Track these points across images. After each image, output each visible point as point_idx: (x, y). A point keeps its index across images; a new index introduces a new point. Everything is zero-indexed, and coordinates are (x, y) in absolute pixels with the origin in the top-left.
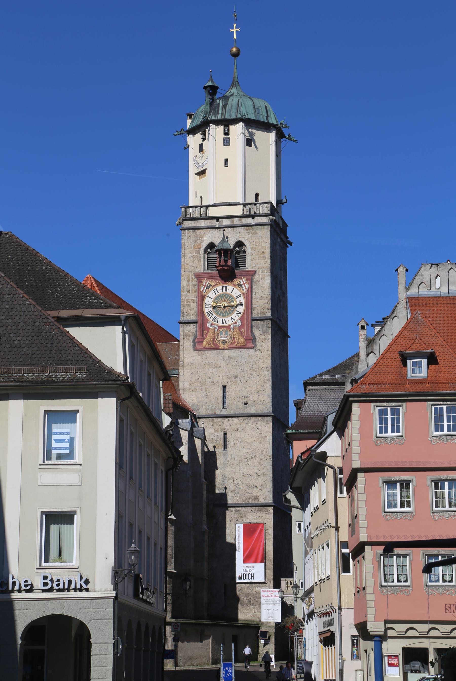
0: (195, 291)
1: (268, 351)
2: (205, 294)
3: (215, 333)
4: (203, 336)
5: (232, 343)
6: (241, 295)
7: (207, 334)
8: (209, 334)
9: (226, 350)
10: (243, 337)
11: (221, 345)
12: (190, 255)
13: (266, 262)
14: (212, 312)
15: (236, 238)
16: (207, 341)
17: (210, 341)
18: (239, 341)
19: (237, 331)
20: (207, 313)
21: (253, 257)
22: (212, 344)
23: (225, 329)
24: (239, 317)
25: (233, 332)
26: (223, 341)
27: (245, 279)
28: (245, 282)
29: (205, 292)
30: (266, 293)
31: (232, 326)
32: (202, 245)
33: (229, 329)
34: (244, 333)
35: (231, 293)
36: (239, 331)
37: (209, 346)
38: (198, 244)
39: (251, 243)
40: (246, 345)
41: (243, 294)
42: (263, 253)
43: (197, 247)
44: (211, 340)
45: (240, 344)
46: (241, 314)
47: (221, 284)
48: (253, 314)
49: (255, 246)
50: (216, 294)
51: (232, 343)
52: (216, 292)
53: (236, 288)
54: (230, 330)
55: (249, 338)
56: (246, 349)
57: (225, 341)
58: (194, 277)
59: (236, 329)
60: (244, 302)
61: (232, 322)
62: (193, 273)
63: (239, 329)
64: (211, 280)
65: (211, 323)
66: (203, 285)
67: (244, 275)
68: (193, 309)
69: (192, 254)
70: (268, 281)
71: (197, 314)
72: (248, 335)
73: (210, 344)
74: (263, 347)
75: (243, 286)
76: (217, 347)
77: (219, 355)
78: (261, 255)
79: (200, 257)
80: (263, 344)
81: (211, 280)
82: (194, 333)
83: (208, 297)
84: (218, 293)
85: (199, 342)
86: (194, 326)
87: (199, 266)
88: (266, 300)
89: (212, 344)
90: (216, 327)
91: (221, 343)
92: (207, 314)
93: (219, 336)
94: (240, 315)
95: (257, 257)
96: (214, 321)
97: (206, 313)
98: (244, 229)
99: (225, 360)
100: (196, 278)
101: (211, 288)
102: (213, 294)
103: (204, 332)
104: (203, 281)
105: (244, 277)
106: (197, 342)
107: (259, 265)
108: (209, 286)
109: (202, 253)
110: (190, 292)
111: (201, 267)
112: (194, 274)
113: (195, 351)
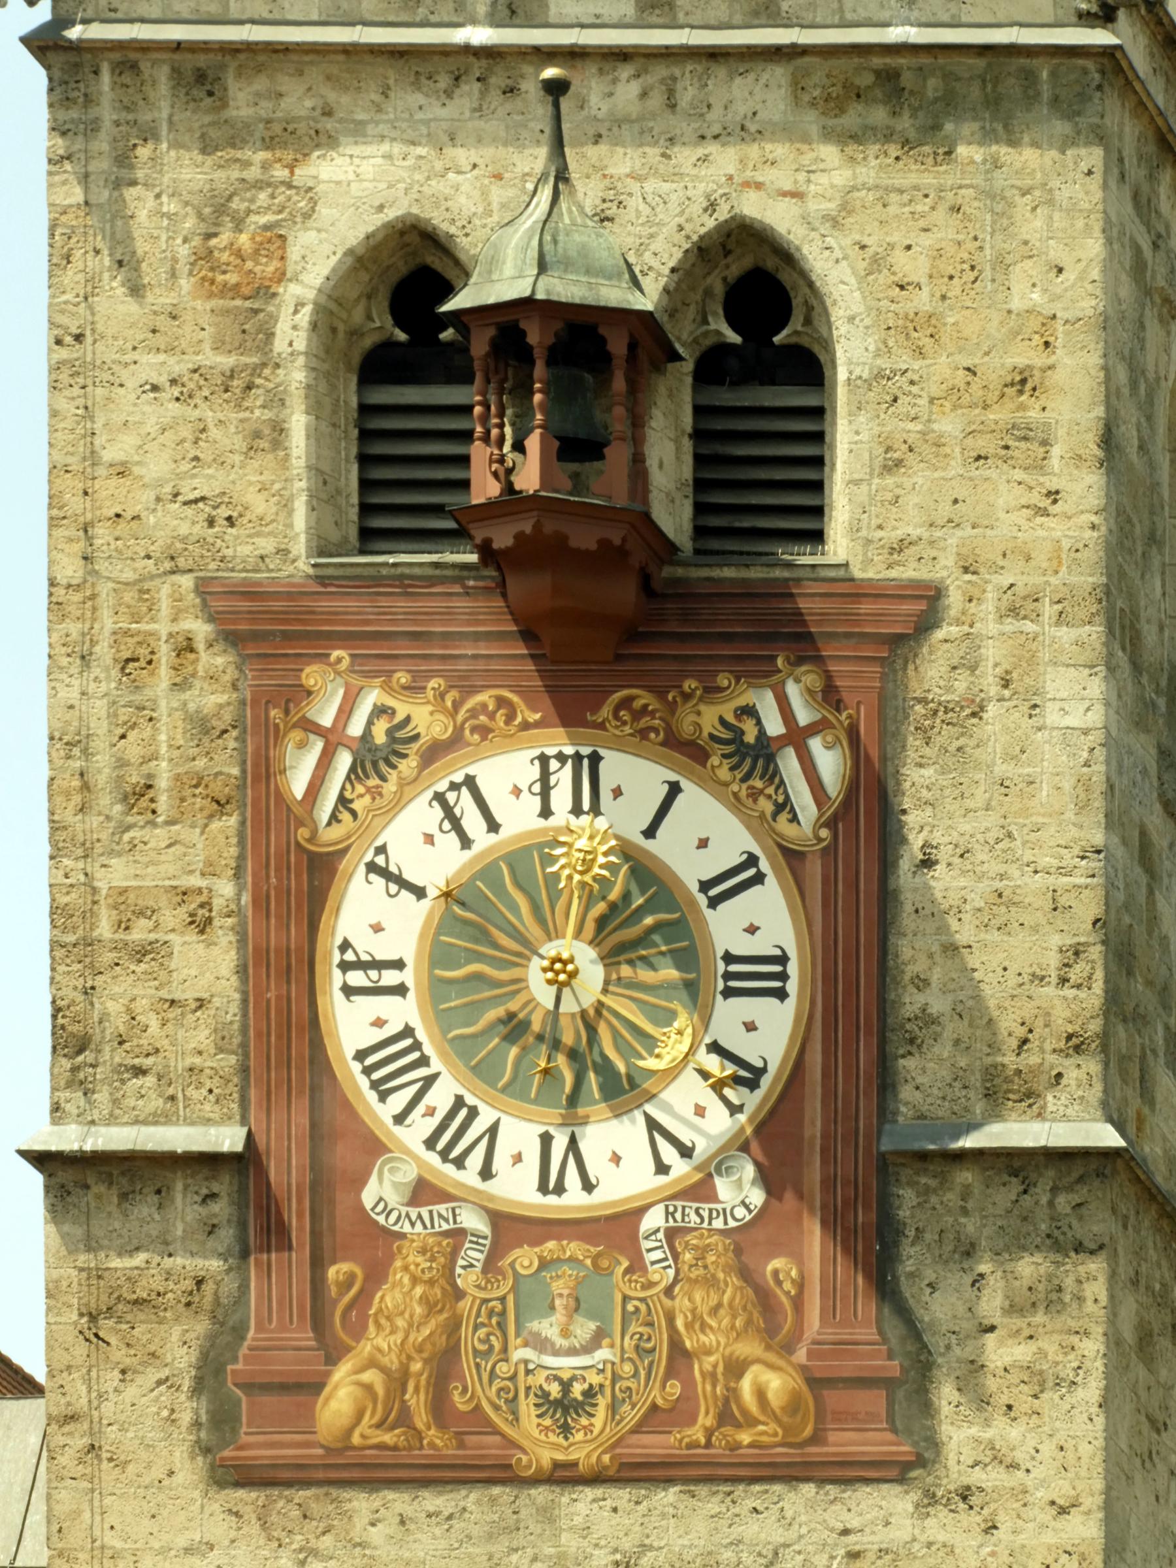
0: (219, 789)
1: (1063, 1511)
2: (336, 832)
3: (459, 1294)
4: (319, 1321)
5: (654, 1407)
6: (764, 865)
8: (388, 1297)
9: (590, 1493)
10: (788, 1348)
13: (1053, 495)
14: (428, 1049)
15: (698, 192)
16: (369, 1376)
17: (398, 1381)
18: (733, 1394)
19: (710, 1282)
20: (360, 1055)
22: (421, 1418)
23: (574, 1248)
25: (669, 1291)
26: (554, 1390)
27: (812, 679)
28: (804, 717)
29: (334, 818)
30: (1046, 861)
31: (654, 1219)
33: (622, 1251)
34: (798, 1302)
35: (650, 833)
36: (735, 1280)
37: (388, 1438)
39: (877, 263)
40: (817, 1438)
42: (1022, 382)
43: (232, 278)
44: (416, 1366)
45: (754, 1422)
46: (766, 1081)
47: (526, 726)
48: (906, 1093)
49: (922, 300)
50: (466, 842)
51: (654, 1407)
52: (473, 822)
53: (701, 782)
54: (637, 1265)
55: (849, 1367)
56: (822, 1482)
57: (577, 1390)
58: (201, 629)
59: (702, 1253)
60: (792, 953)
61: (662, 1168)
62: (186, 582)
63: (738, 1251)
64: (403, 678)
65: (408, 1174)
66: (317, 730)
68: (201, 1003)
69: (170, 350)
70: (1073, 721)
71: (244, 1070)
73: (404, 1419)
74: (1013, 1466)
75: (789, 764)
76: (486, 1446)
78: (1000, 415)
79: (277, 400)
80: (1014, 1433)
81: (403, 678)
82: (209, 1288)
83: (372, 867)
84: (493, 826)
85: (267, 1388)
86: (215, 1207)
87: (260, 505)
88: (1056, 940)
89: (421, 1418)
90: (472, 1220)
91: (527, 1408)
92: (367, 1071)
93: (501, 1326)
95: (949, 425)
96: (444, 1155)
97: (349, 1053)
98: (798, 87)
100: (231, 638)
101: (408, 766)
104: (311, 676)
105: (800, 661)
106: (249, 1387)
107: (969, 531)
108: (380, 737)
109: (301, 345)
110: (163, 803)
111: (291, 513)
112: (203, 588)
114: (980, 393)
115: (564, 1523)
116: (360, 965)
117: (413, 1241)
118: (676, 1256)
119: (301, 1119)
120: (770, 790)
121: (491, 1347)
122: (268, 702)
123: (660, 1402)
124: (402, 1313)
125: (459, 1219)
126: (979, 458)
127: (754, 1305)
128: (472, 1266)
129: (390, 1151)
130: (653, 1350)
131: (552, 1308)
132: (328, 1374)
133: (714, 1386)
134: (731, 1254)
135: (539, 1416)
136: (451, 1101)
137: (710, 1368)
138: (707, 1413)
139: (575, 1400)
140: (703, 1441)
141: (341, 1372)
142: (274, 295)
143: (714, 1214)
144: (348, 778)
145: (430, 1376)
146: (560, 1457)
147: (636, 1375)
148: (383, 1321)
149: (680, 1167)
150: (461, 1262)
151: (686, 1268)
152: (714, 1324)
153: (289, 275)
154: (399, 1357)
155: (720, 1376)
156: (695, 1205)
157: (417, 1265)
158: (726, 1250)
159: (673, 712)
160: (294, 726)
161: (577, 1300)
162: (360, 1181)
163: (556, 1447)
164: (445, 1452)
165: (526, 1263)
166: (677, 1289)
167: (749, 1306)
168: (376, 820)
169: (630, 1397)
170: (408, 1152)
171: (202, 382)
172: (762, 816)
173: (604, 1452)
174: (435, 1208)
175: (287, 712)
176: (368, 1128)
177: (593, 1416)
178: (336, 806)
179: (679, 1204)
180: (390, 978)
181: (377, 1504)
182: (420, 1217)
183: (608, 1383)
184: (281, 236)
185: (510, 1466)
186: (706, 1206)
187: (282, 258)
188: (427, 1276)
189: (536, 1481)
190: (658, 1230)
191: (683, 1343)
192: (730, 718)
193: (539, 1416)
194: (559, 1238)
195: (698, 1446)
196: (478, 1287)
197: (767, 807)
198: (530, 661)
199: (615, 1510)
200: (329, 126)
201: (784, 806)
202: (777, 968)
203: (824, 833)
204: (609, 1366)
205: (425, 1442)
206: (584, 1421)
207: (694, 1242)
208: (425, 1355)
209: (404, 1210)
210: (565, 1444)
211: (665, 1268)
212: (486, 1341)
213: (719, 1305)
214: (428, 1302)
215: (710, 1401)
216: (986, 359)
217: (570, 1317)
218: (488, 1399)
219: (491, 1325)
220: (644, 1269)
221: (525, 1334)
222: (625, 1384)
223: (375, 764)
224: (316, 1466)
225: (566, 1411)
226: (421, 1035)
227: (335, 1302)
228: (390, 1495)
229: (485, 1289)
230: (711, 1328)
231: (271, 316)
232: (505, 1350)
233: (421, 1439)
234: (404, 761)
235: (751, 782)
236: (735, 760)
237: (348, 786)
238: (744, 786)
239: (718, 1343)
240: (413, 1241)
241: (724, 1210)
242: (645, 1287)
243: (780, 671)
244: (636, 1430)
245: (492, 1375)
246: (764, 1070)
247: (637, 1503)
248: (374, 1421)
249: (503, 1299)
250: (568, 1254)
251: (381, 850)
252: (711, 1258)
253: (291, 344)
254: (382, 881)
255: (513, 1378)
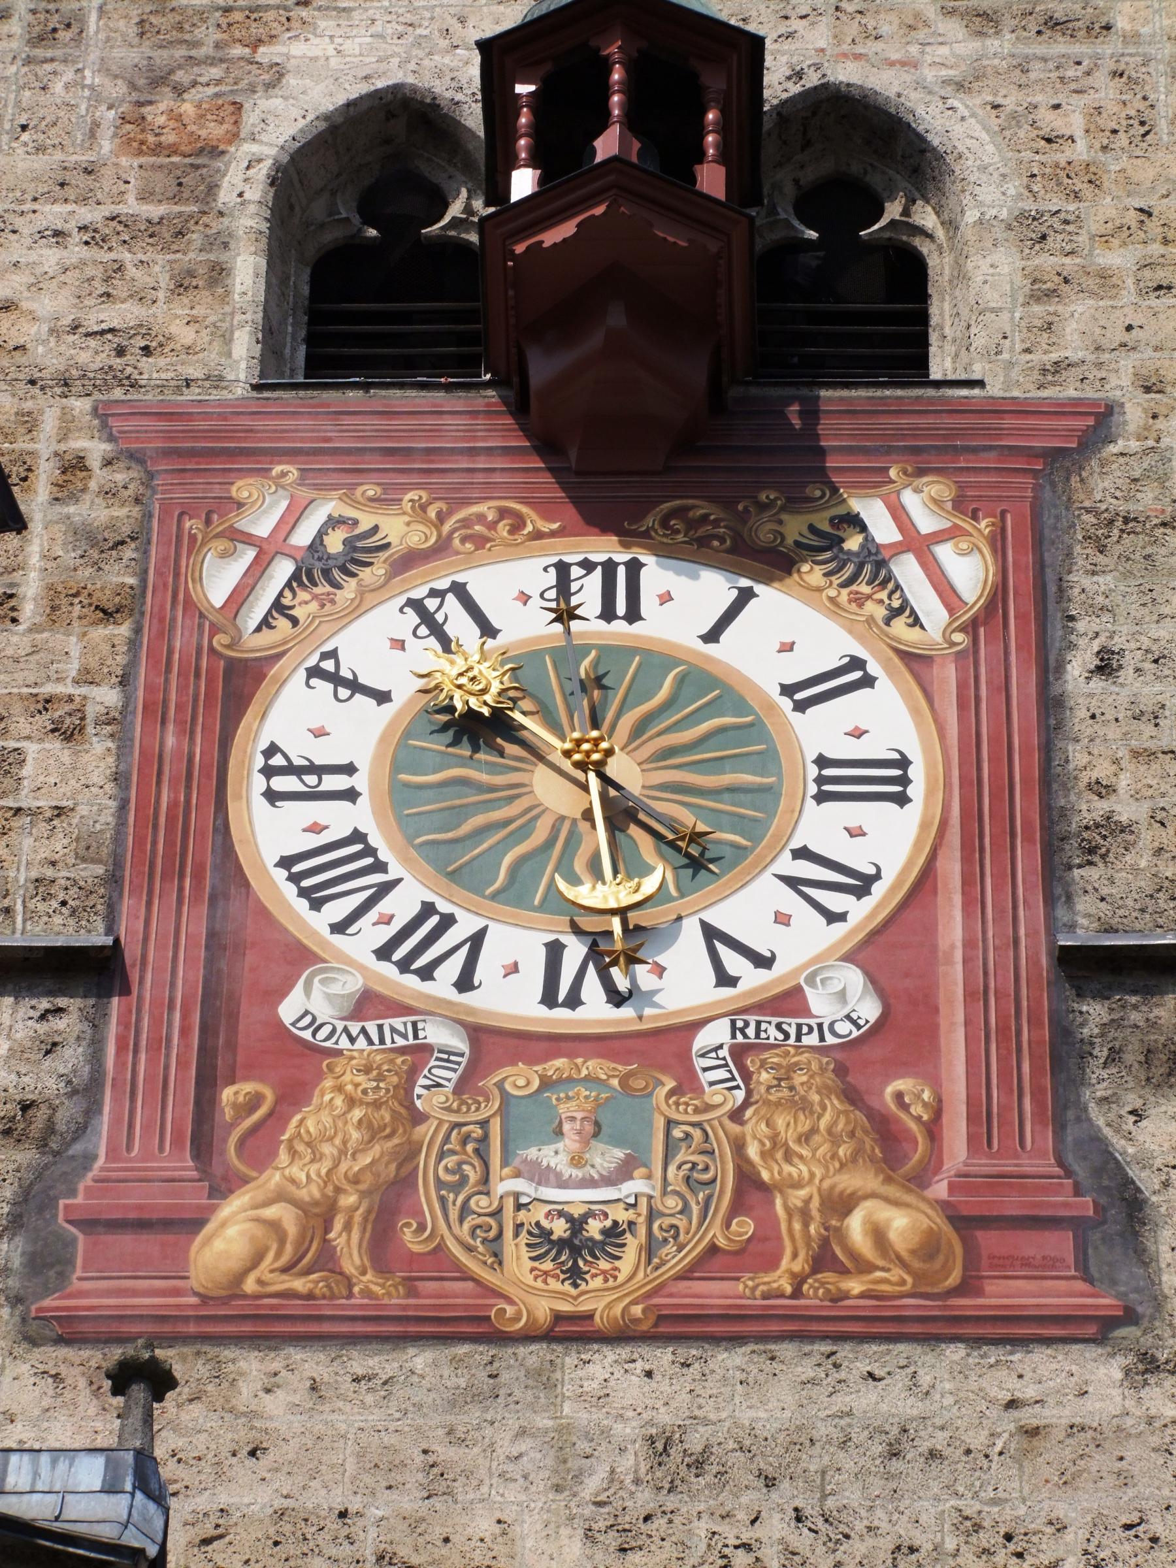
2: (267, 638)
3: (418, 1118)
5: (713, 1249)
7: (277, 1118)
9: (610, 1354)
11: (529, 1279)
12: (53, 214)
16: (271, 1212)
20: (286, 862)
21: (1047, 262)
23: (593, 1066)
24: (839, 929)
25: (736, 1115)
27: (939, 488)
29: (265, 623)
31: (717, 1034)
32: (250, 119)
33: (664, 1069)
35: (712, 636)
37: (300, 1285)
38: (188, 109)
41: (903, 655)
43: (169, 138)
44: (349, 1200)
45: (863, 1267)
46: (878, 889)
49: (1081, 151)
51: (713, 1249)
54: (688, 1083)
57: (594, 1228)
61: (725, 979)
63: (841, 1070)
65: (352, 984)
66: (248, 539)
67: (916, 451)
72: (999, 1155)
73: (327, 1260)
75: (907, 570)
77: (474, 1414)
91: (517, 1253)
92: (295, 878)
93: (482, 1155)
94: (859, 910)
97: (270, 858)
99: (593, 1484)
102: (400, 645)
103: (227, 1094)
113: (33, 1341)
114: (1160, 230)
115: (568, 1389)
116: (290, 769)
117: (352, 1058)
118: (747, 1076)
119: (195, 922)
120: (883, 595)
121: (464, 1179)
122: (181, 514)
123: (722, 1242)
124: (331, 1139)
125: (421, 1034)
126: (1160, 287)
127: (866, 1132)
128: (439, 1085)
129: (324, 961)
130: (714, 1180)
131: (559, 1133)
132: (213, 1209)
133: (806, 1225)
134: (830, 1075)
135: (532, 1259)
136: (416, 909)
137: (799, 1204)
138: (795, 1255)
139: (591, 1239)
140: (789, 1289)
141: (234, 1205)
142: (223, 153)
143: (805, 1029)
144: (288, 585)
145: (369, 1212)
146: (565, 1307)
147: (685, 1210)
148: (300, 1147)
149: (751, 978)
150: (422, 1081)
151: (763, 1089)
152: (805, 1152)
153: (242, 135)
154: (322, 1190)
155: (815, 1213)
156: (775, 1020)
157: (357, 1085)
158: (823, 1070)
159: (744, 522)
160: (217, 536)
161: (597, 1124)
162: (282, 992)
163: (563, 1296)
164: (386, 1301)
165: (521, 1082)
166: (749, 1113)
167: (859, 1133)
168: (324, 627)
169: (675, 1237)
170: (351, 962)
171: (120, 228)
172: (870, 620)
173: (635, 1302)
174: (387, 1023)
175: (208, 522)
176: (294, 937)
177: (619, 1258)
178: (269, 612)
179: (752, 1019)
180: (333, 783)
181: (276, 1365)
182: (364, 1031)
183: (641, 1220)
184: (235, 103)
185: (488, 1318)
186: (794, 1021)
187: (236, 122)
188: (371, 1097)
189: (527, 1337)
190: (721, 1047)
191: (759, 1173)
192: (826, 527)
193: (532, 1259)
194: (571, 1055)
195: (782, 1296)
196: (449, 1109)
197: (880, 612)
198: (548, 475)
199: (649, 1374)
200: (304, 14)
201: (903, 610)
202: (896, 772)
203: (958, 637)
204: (643, 1202)
205: (356, 1289)
206: (604, 1265)
207: (775, 1060)
208: (363, 1187)
209: (340, 1025)
210: (573, 1292)
211: (730, 1089)
212: (458, 1169)
213: (814, 1130)
214: (370, 1126)
215: (800, 1243)
216: (1166, 201)
217: (586, 1143)
218: (457, 1238)
219: (465, 1153)
220: (698, 1090)
221: (516, 1162)
222: (668, 1221)
223: (326, 573)
224: (186, 1319)
225: (576, 1252)
226: (375, 840)
227: (233, 1125)
228: (296, 1354)
229: (458, 1111)
230: (801, 1157)
231: (218, 171)
232: (485, 1180)
233: (350, 1286)
234: (368, 570)
235: (854, 587)
236: (832, 566)
237: (287, 593)
238: (845, 592)
239: (812, 1175)
240: (352, 1058)
241: (820, 1026)
242: (697, 1111)
243: (894, 482)
244: (685, 1275)
245: (465, 1211)
246: (877, 877)
247: (686, 1365)
248: (277, 1265)
249: (484, 1124)
250: (584, 1072)
251: (333, 654)
252: (799, 1078)
253: (240, 195)
254: (331, 686)
255: (497, 1213)
